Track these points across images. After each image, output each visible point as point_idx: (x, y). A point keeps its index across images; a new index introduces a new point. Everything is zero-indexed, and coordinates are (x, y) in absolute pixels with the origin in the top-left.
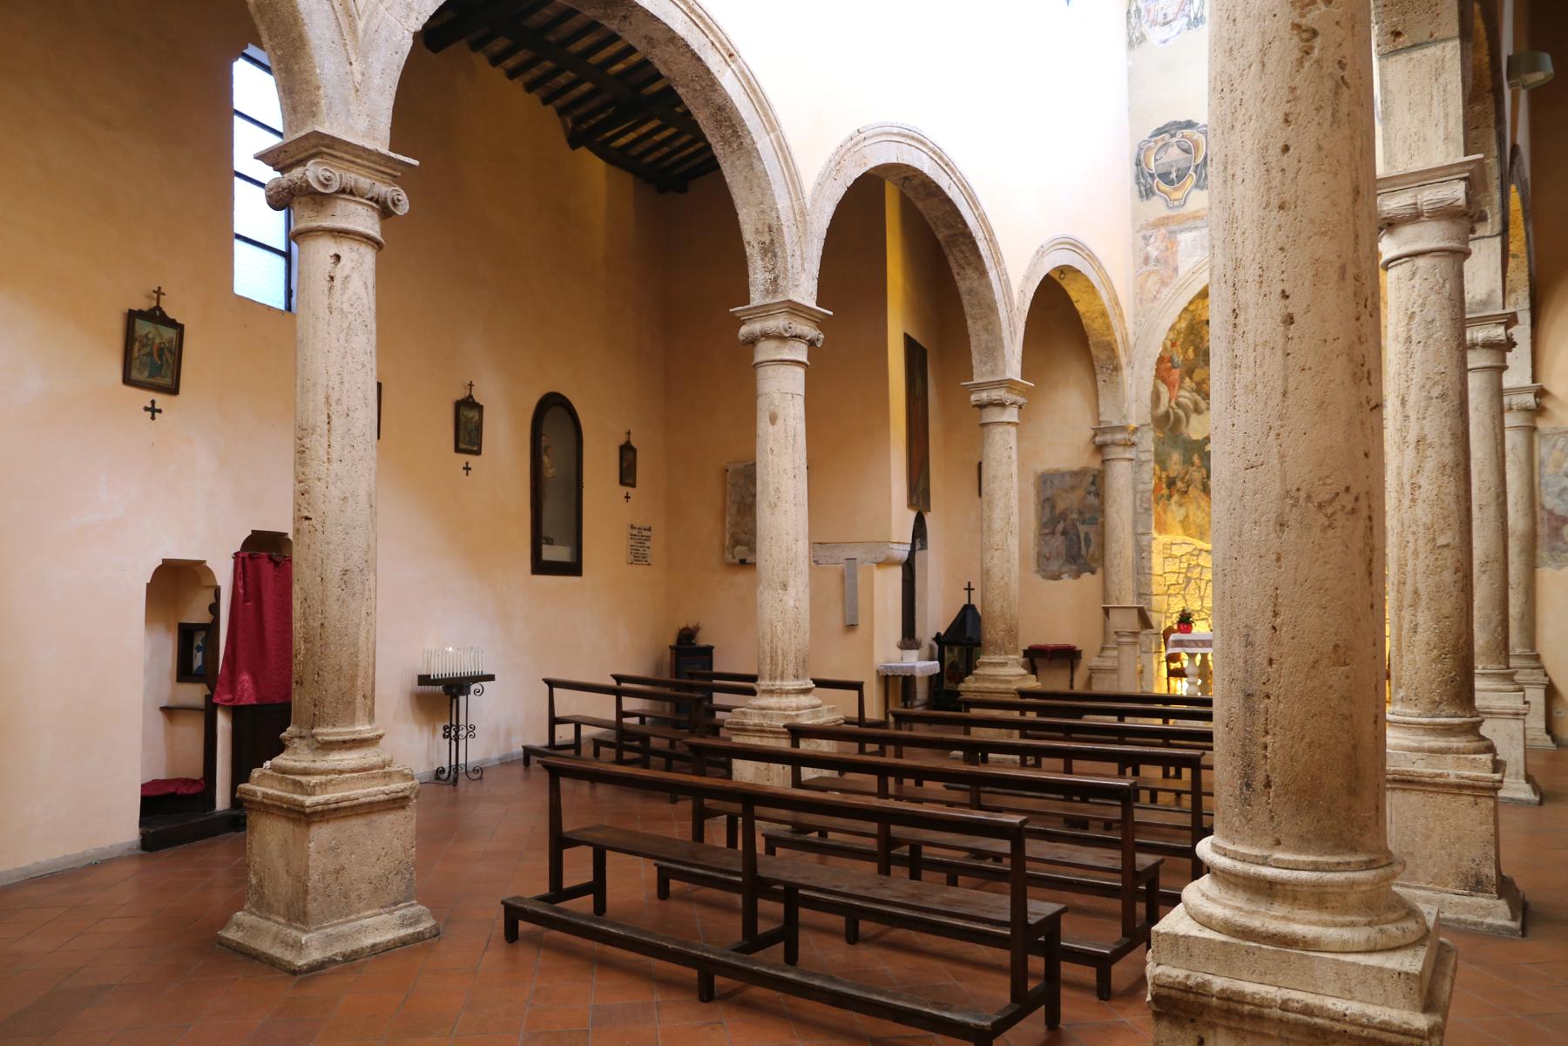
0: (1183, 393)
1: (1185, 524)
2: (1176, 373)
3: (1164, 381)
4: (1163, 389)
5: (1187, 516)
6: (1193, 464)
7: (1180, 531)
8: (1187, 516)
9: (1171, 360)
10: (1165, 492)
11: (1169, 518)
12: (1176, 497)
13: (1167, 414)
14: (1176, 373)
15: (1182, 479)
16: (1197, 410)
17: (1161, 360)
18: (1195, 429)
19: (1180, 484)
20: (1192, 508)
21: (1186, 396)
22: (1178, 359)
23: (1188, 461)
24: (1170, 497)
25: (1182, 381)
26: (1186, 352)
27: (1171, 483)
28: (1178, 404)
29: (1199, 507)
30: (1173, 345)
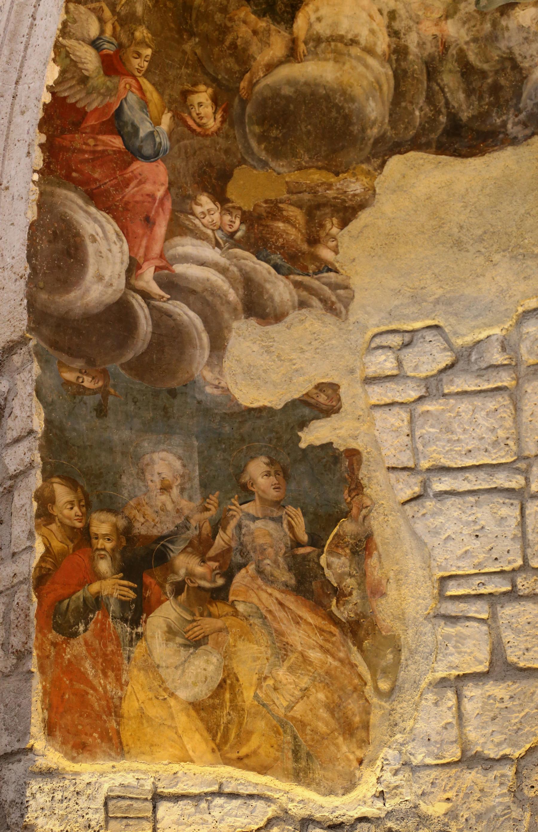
0: (187, 246)
1: (220, 719)
2: (153, 179)
3: (96, 197)
4: (96, 227)
5: (227, 684)
6: (246, 493)
7: (196, 742)
8: (227, 684)
9: (117, 123)
10: (112, 586)
11: (137, 694)
12: (168, 613)
13: (119, 314)
14: (153, 179)
15: (201, 547)
16: (256, 306)
17: (60, 118)
18: (256, 368)
19: (185, 563)
20: (251, 657)
21: (202, 259)
22: (155, 124)
23: (223, 481)
24: (136, 612)
25: (182, 204)
26: (180, 104)
27: (143, 559)
28: (172, 285)
29: (282, 650)
30: (113, 65)
